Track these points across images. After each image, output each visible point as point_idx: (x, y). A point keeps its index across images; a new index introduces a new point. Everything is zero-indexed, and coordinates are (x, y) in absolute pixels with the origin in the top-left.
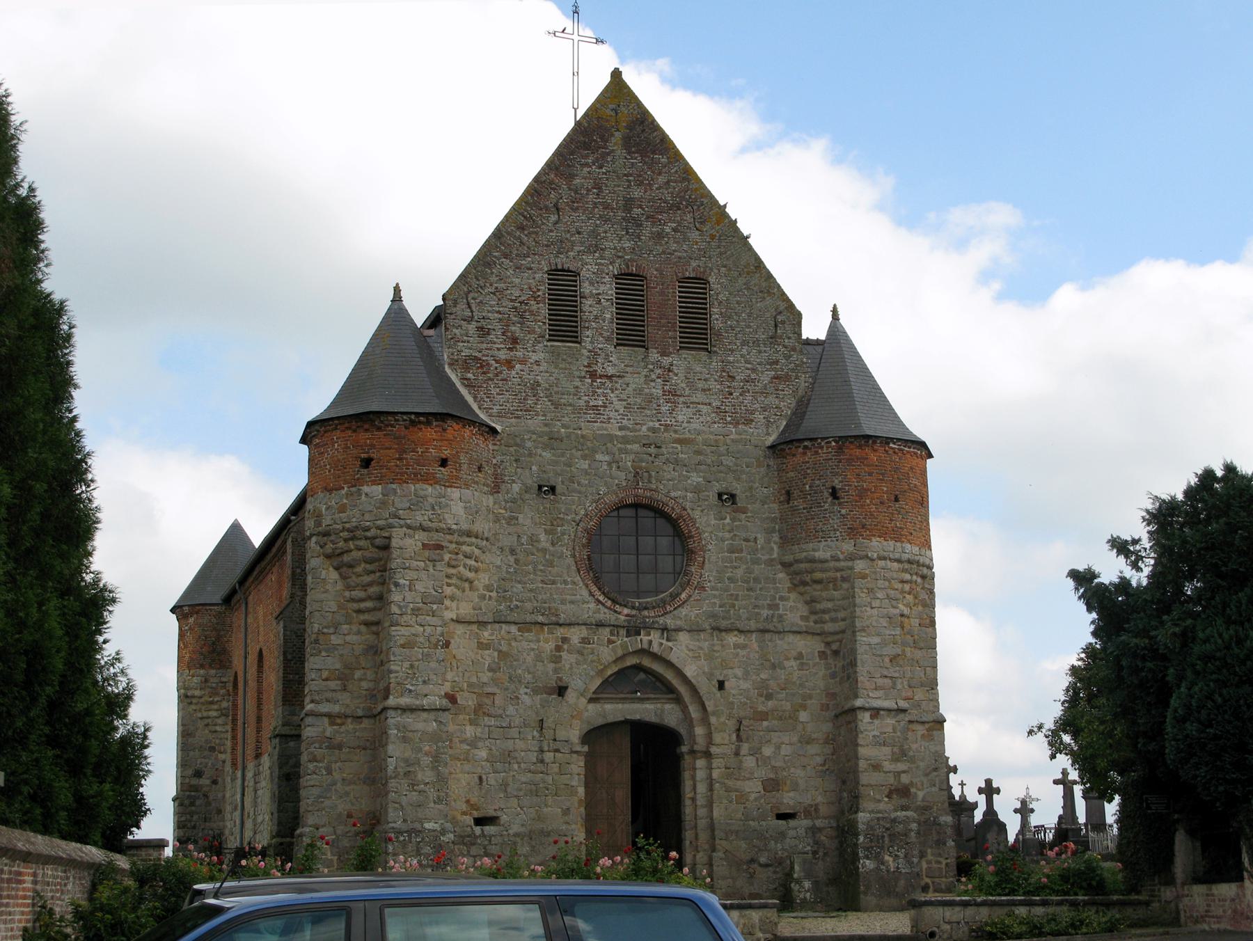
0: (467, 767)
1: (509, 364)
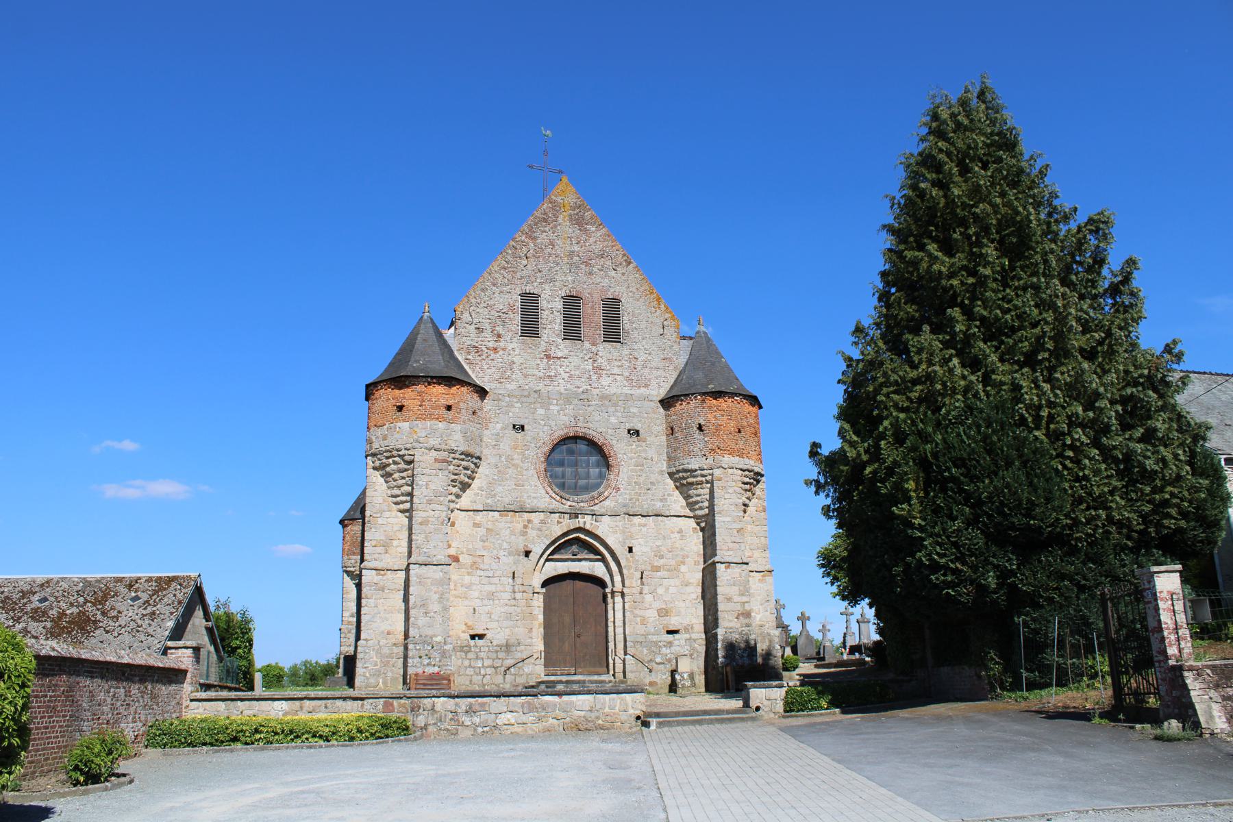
0: (466, 603)
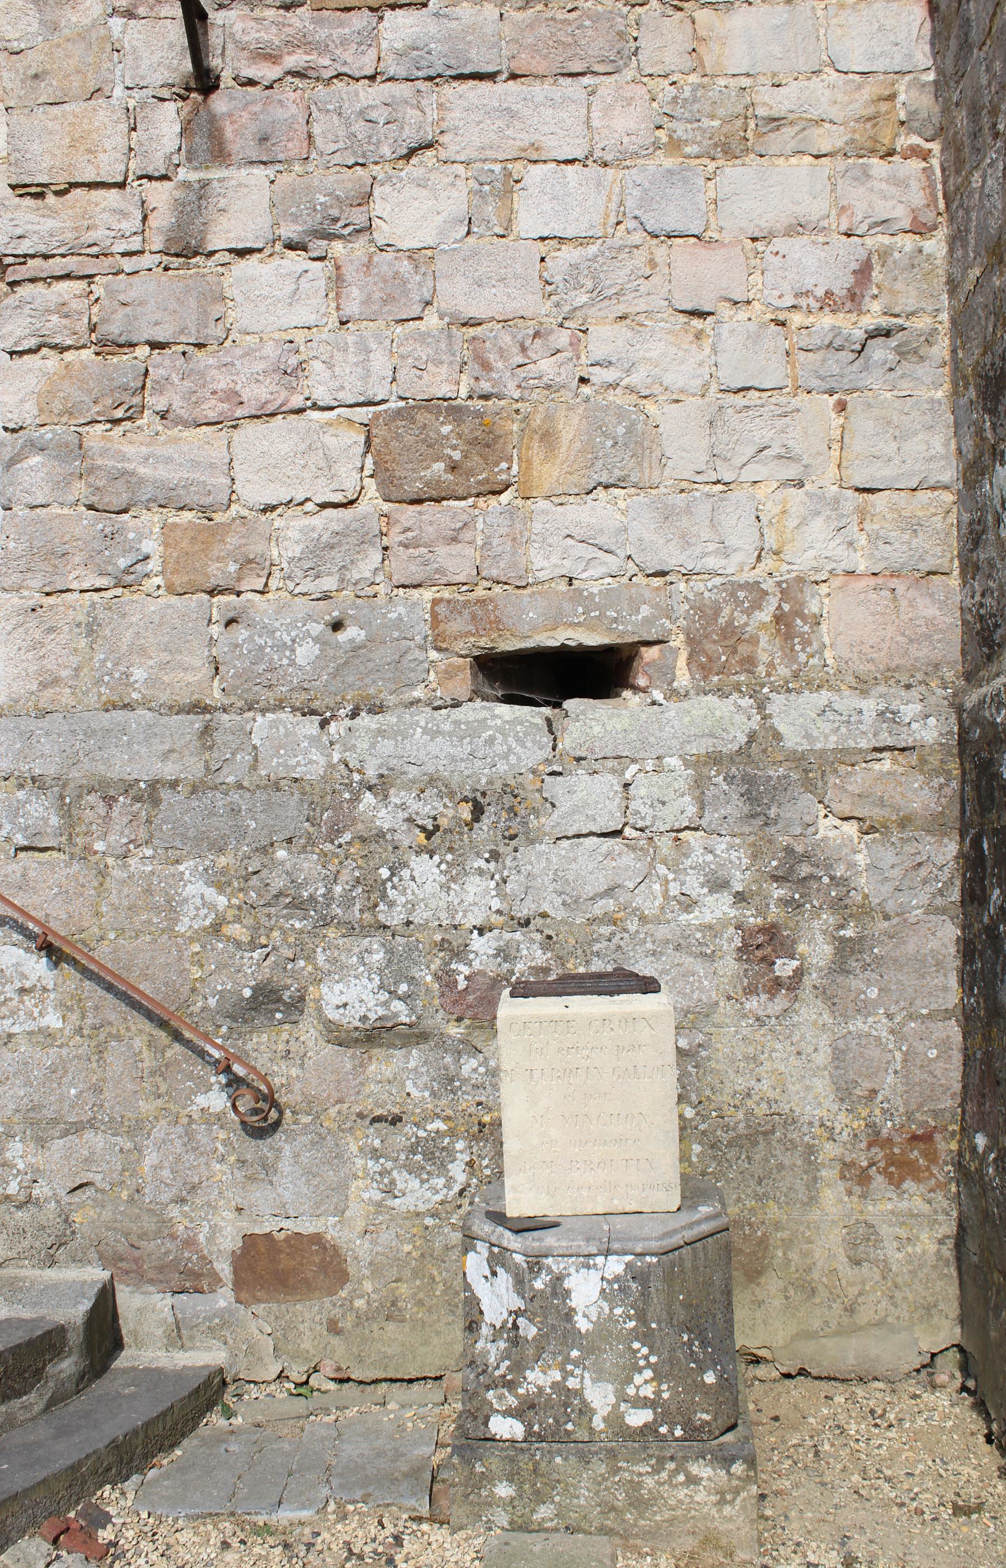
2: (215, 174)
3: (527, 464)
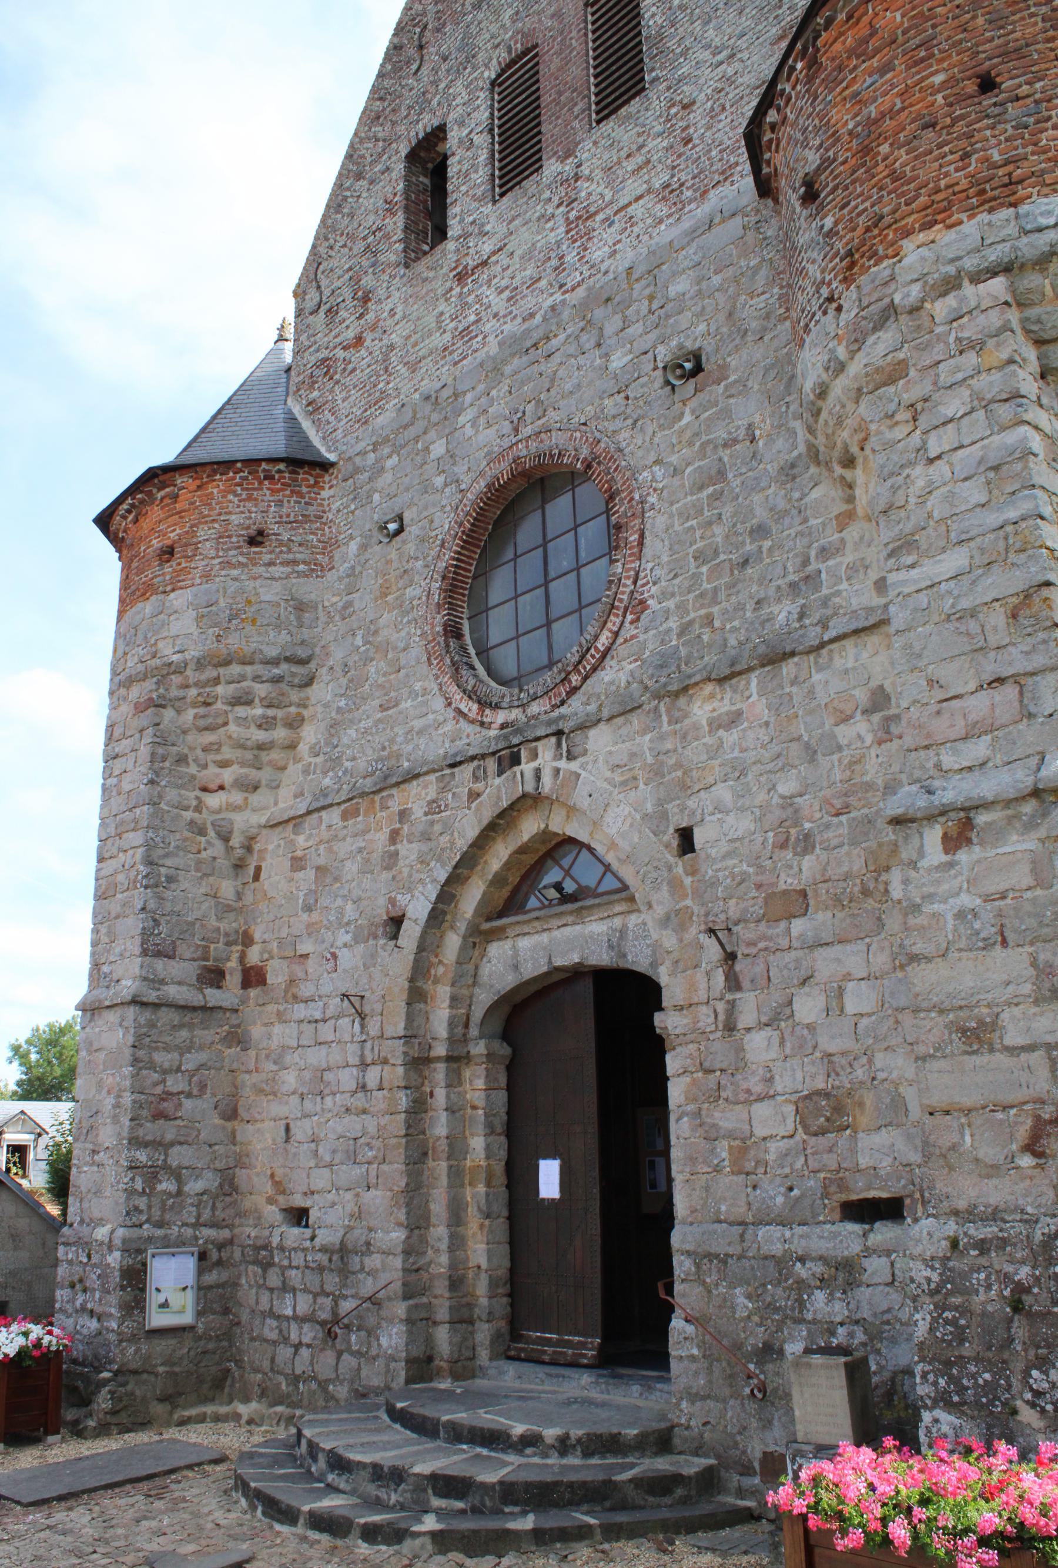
1: (359, 340)
2: (738, 995)
3: (854, 1118)
